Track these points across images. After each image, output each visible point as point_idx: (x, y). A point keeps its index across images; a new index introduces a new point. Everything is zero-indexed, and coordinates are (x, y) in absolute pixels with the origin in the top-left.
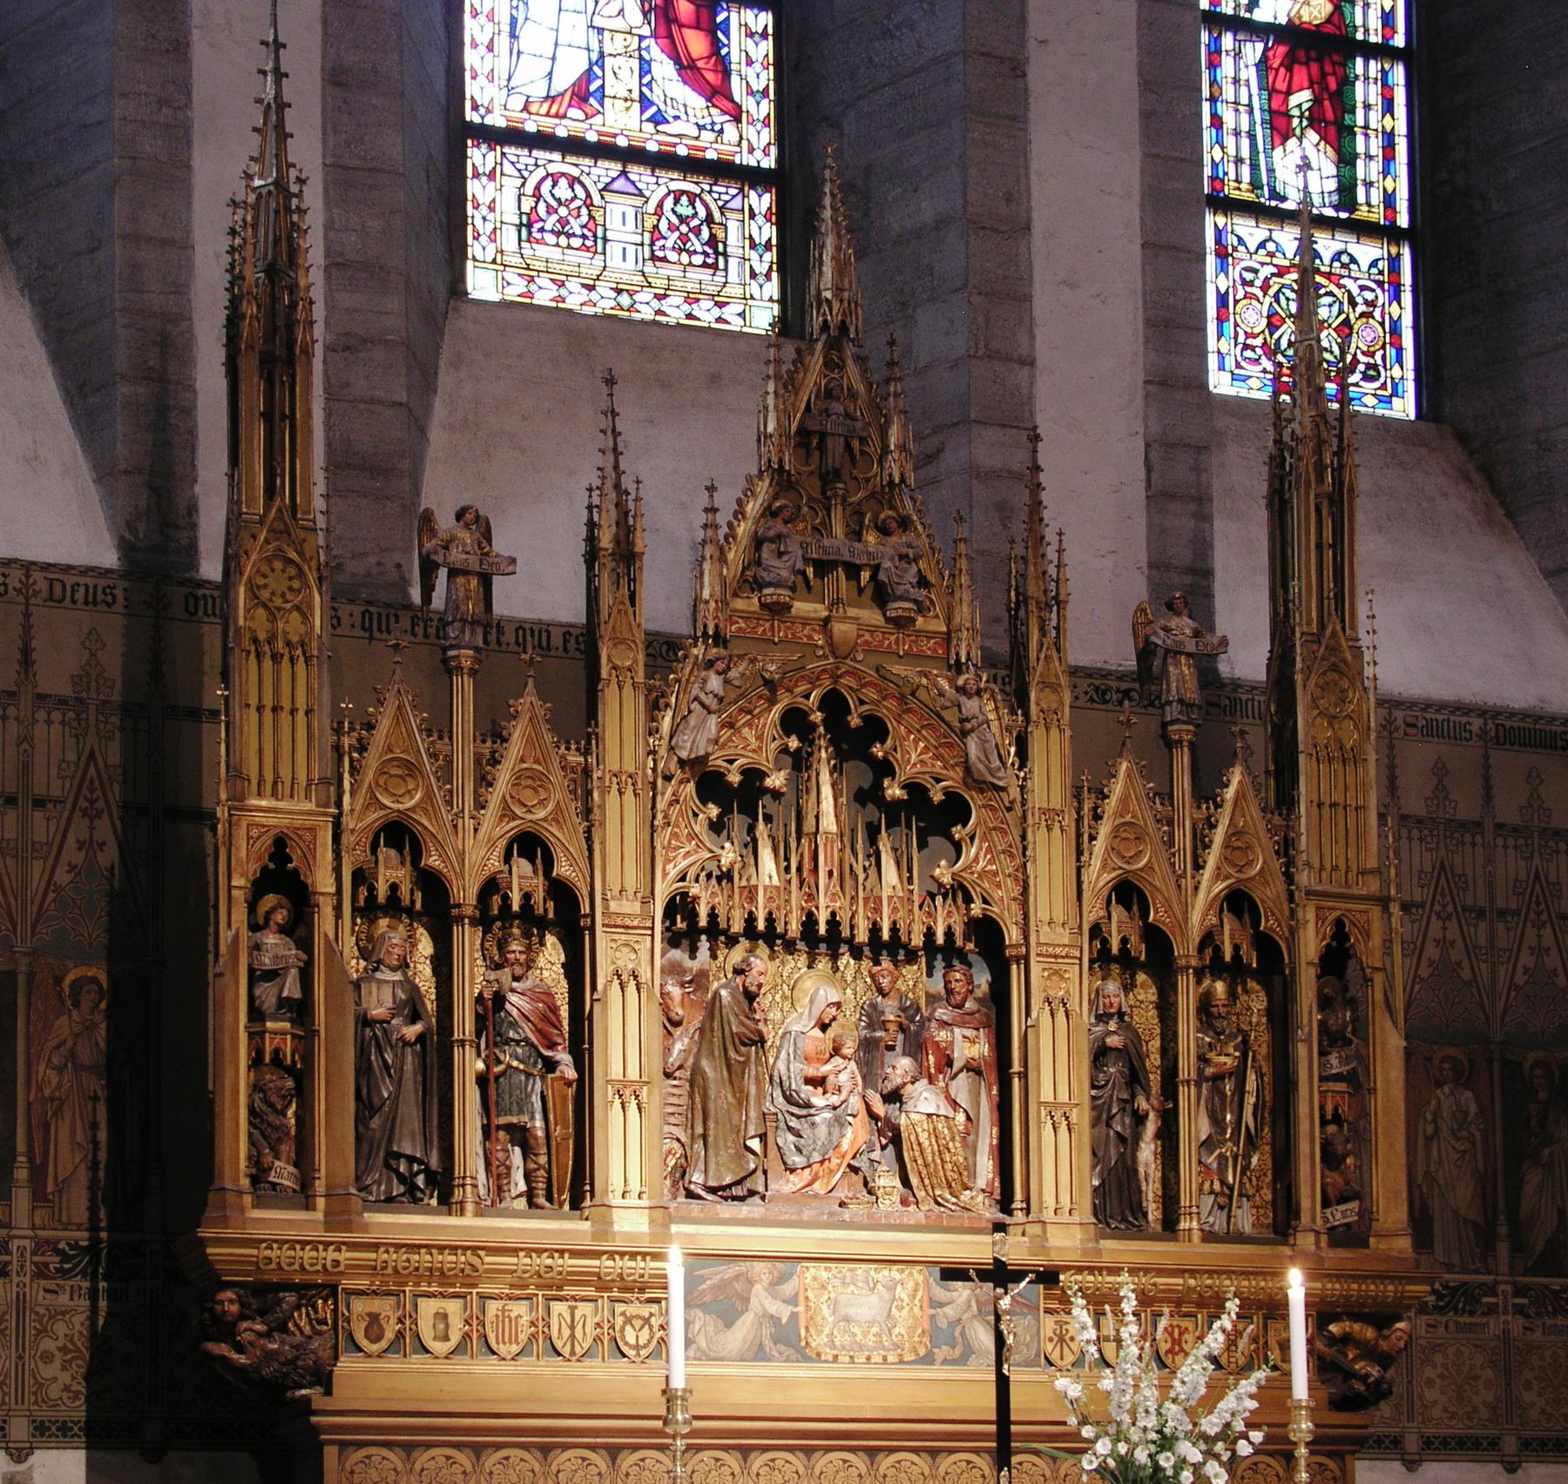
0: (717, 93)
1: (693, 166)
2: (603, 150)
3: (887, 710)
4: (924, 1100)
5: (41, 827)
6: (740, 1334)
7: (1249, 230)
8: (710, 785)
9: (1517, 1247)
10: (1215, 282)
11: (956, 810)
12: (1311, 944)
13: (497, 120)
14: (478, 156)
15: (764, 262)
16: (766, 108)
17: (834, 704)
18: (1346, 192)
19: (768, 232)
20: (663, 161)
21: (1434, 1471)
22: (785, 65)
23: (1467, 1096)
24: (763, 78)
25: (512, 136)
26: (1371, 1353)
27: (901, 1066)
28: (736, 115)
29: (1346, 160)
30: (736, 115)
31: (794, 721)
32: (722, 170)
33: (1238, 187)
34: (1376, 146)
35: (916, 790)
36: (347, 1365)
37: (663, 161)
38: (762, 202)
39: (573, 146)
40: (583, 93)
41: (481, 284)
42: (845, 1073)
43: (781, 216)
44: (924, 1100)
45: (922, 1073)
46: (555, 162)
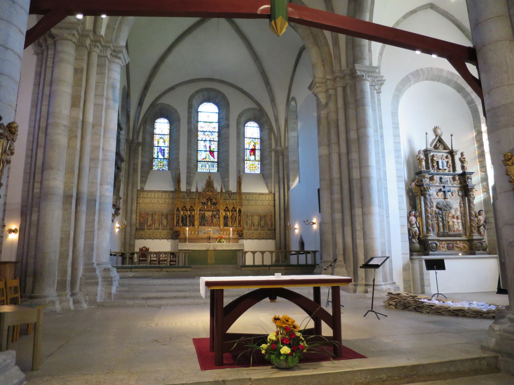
0: (214, 157)
1: (212, 162)
2: (207, 161)
3: (212, 198)
4: (215, 220)
5: (170, 205)
6: (202, 233)
7: (248, 162)
8: (202, 203)
9: (260, 226)
10: (246, 165)
11: (216, 203)
12: (238, 210)
13: (200, 160)
14: (199, 163)
15: (216, 167)
16: (217, 158)
17: (209, 198)
18: (255, 159)
19: (217, 165)
20: (210, 162)
21: (247, 240)
22: (218, 155)
23: (257, 217)
24: (217, 156)
25: (201, 161)
26: (241, 233)
27: (213, 218)
28: (215, 158)
29: (255, 157)
30: (215, 158)
31: (207, 199)
32: (214, 162)
33: (248, 159)
34: (257, 156)
35: (214, 203)
36: (180, 235)
37: (210, 162)
38: (216, 163)
39: (205, 161)
40: (205, 158)
41: (199, 171)
42: (210, 218)
43: (217, 164)
44: (215, 220)
45: (214, 218)
46: (203, 162)
